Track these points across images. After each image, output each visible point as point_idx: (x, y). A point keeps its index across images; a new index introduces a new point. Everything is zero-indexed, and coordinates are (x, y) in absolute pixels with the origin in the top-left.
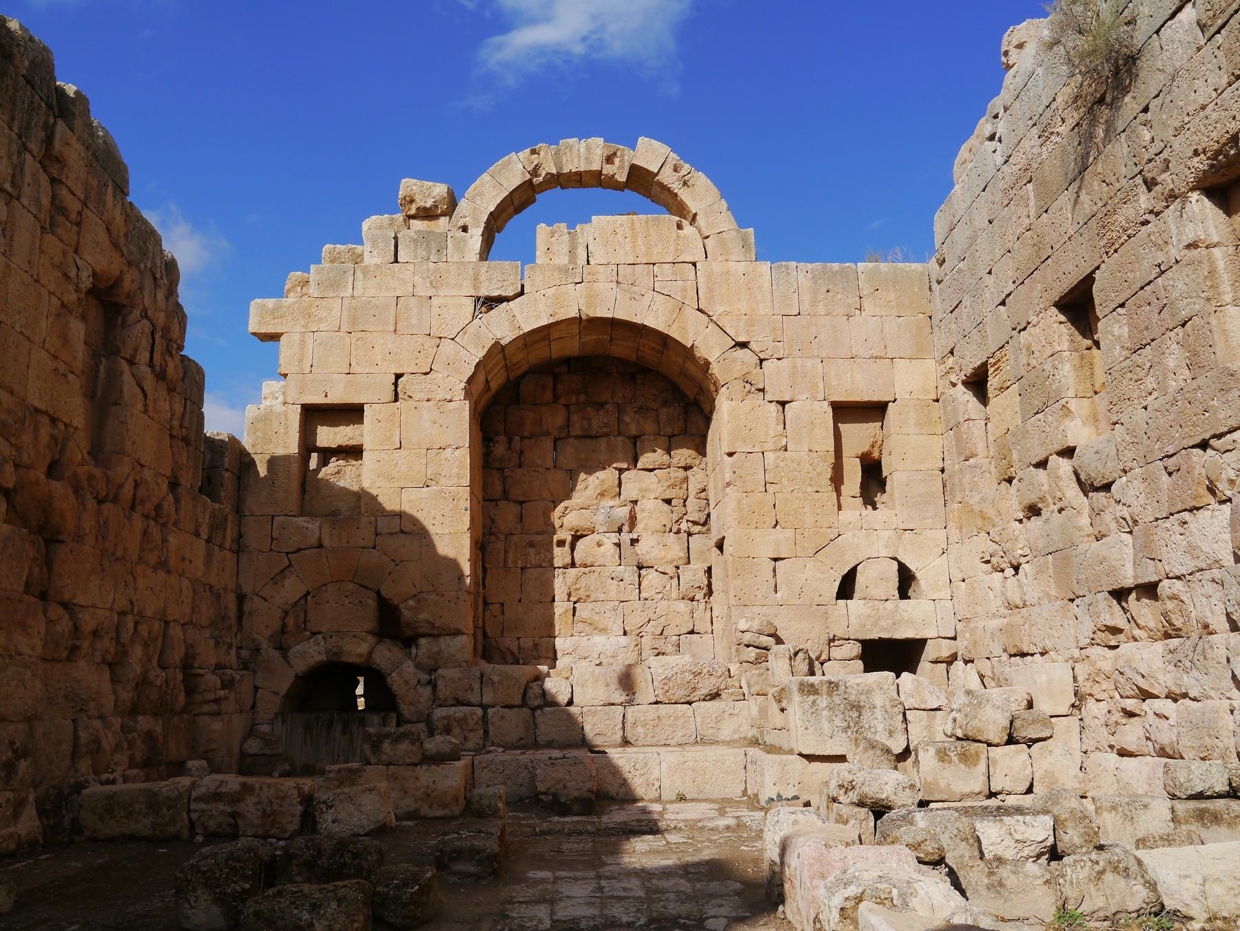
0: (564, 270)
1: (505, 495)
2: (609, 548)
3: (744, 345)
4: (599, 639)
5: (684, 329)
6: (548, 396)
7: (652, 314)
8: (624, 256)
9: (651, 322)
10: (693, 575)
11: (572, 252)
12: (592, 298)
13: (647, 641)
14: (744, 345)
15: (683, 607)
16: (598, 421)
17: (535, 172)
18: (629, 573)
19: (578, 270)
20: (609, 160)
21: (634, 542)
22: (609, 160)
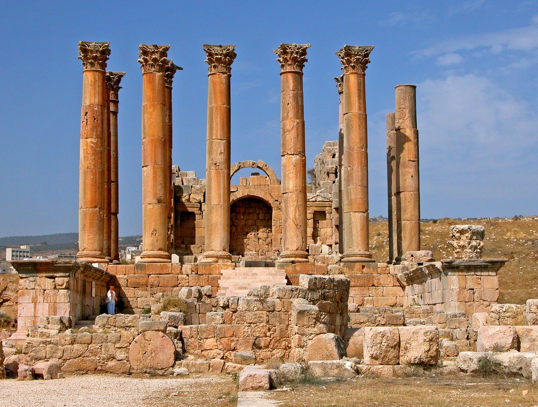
0: (245, 186)
1: (233, 225)
2: (253, 235)
3: (277, 201)
4: (251, 252)
5: (266, 198)
6: (241, 205)
7: (260, 194)
8: (256, 183)
9: (260, 196)
10: (269, 240)
11: (246, 183)
12: (250, 191)
13: (260, 253)
14: (277, 201)
15: (266, 246)
16: (251, 211)
17: (240, 167)
18: (256, 240)
19: (247, 186)
20: (253, 165)
21: (258, 234)
22: (253, 165)
